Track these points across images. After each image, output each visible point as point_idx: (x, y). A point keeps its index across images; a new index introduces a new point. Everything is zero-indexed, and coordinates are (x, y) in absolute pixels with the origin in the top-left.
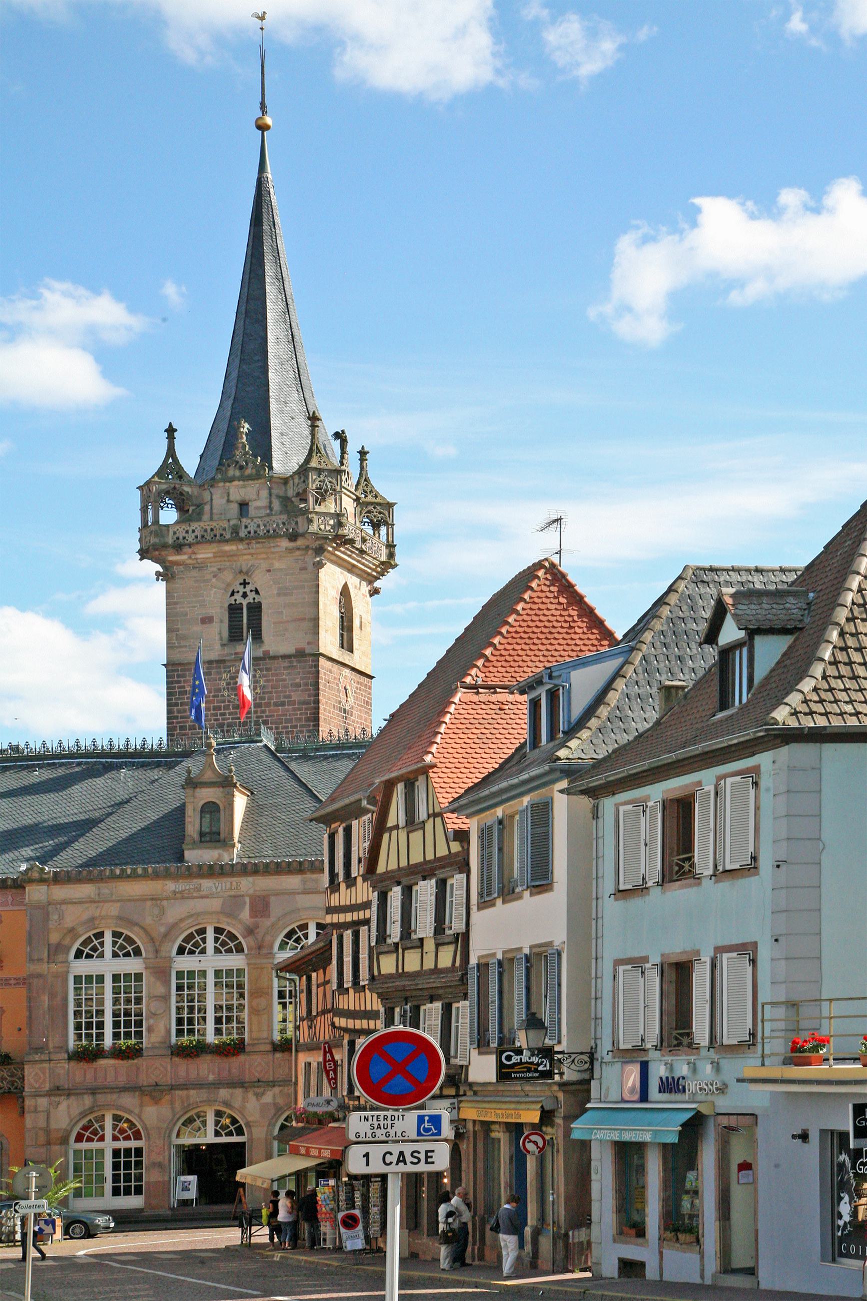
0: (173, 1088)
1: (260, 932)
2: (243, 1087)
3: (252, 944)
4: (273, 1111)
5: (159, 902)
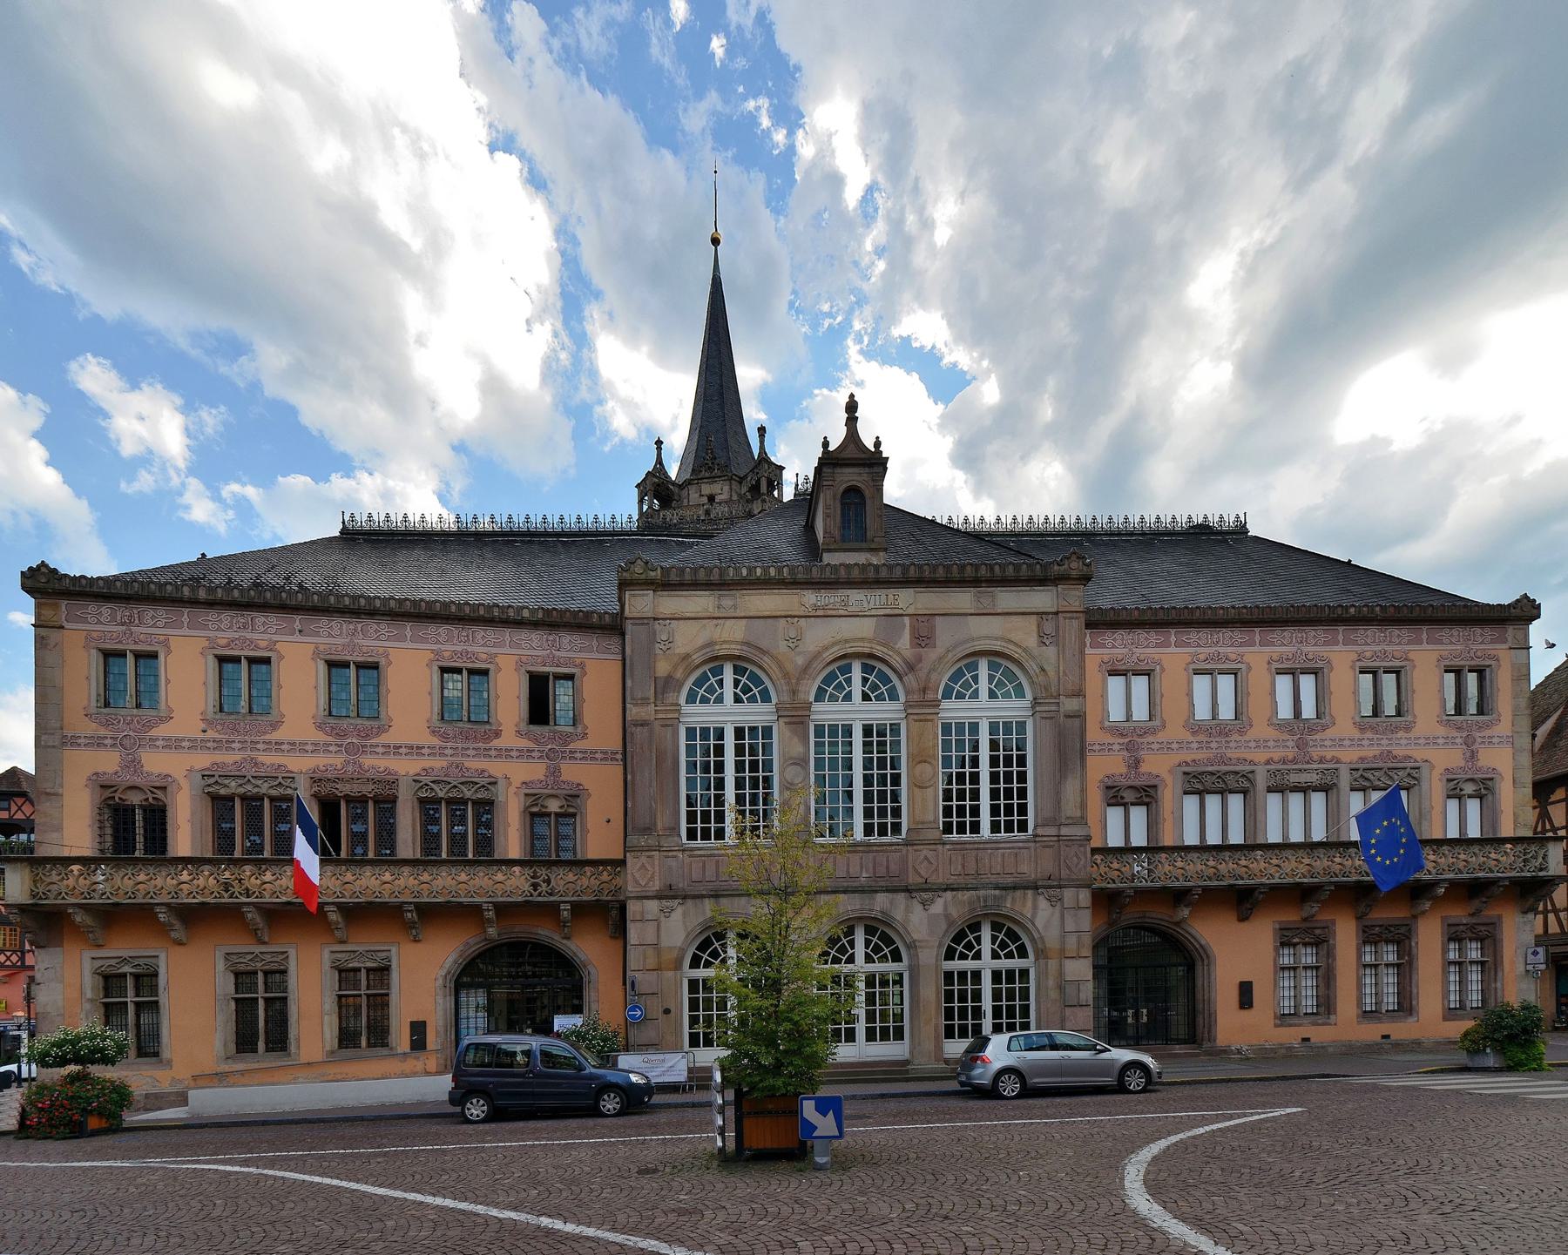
1: (925, 667)
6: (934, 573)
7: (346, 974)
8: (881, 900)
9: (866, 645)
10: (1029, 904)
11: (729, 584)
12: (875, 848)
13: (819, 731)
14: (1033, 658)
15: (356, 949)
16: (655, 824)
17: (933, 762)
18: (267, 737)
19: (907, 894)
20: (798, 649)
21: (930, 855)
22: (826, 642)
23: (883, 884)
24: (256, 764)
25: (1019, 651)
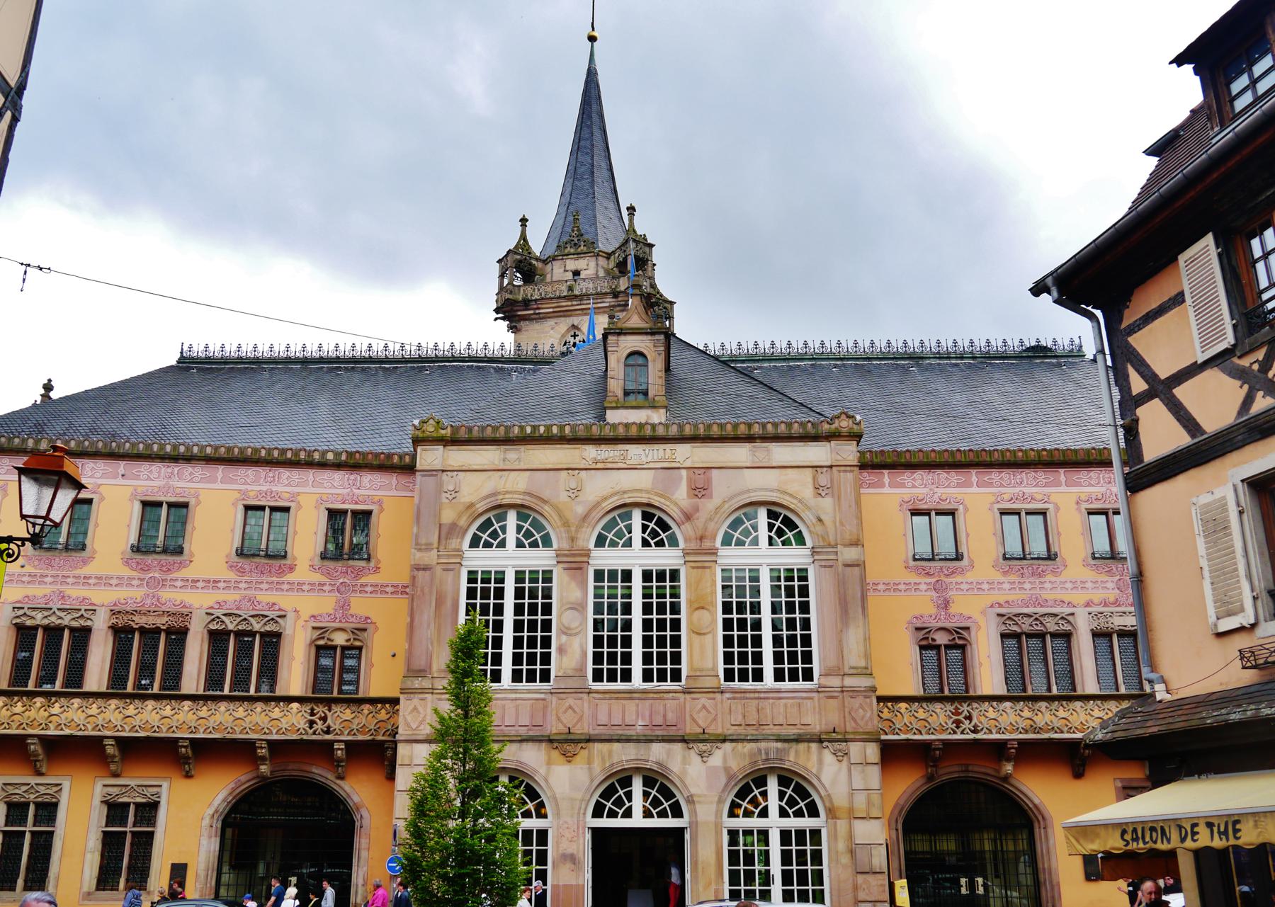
0: (589, 740)
1: (701, 518)
2: (683, 740)
3: (691, 533)
4: (723, 780)
5: (577, 471)
6: (709, 430)
7: (115, 811)
8: (656, 754)
9: (644, 495)
10: (814, 757)
11: (514, 441)
12: (651, 695)
13: (599, 575)
14: (809, 508)
15: (128, 783)
16: (430, 667)
17: (711, 608)
18: (77, 572)
19: (684, 745)
20: (578, 499)
21: (709, 703)
22: (605, 493)
23: (659, 733)
24: (63, 597)
25: (795, 502)
